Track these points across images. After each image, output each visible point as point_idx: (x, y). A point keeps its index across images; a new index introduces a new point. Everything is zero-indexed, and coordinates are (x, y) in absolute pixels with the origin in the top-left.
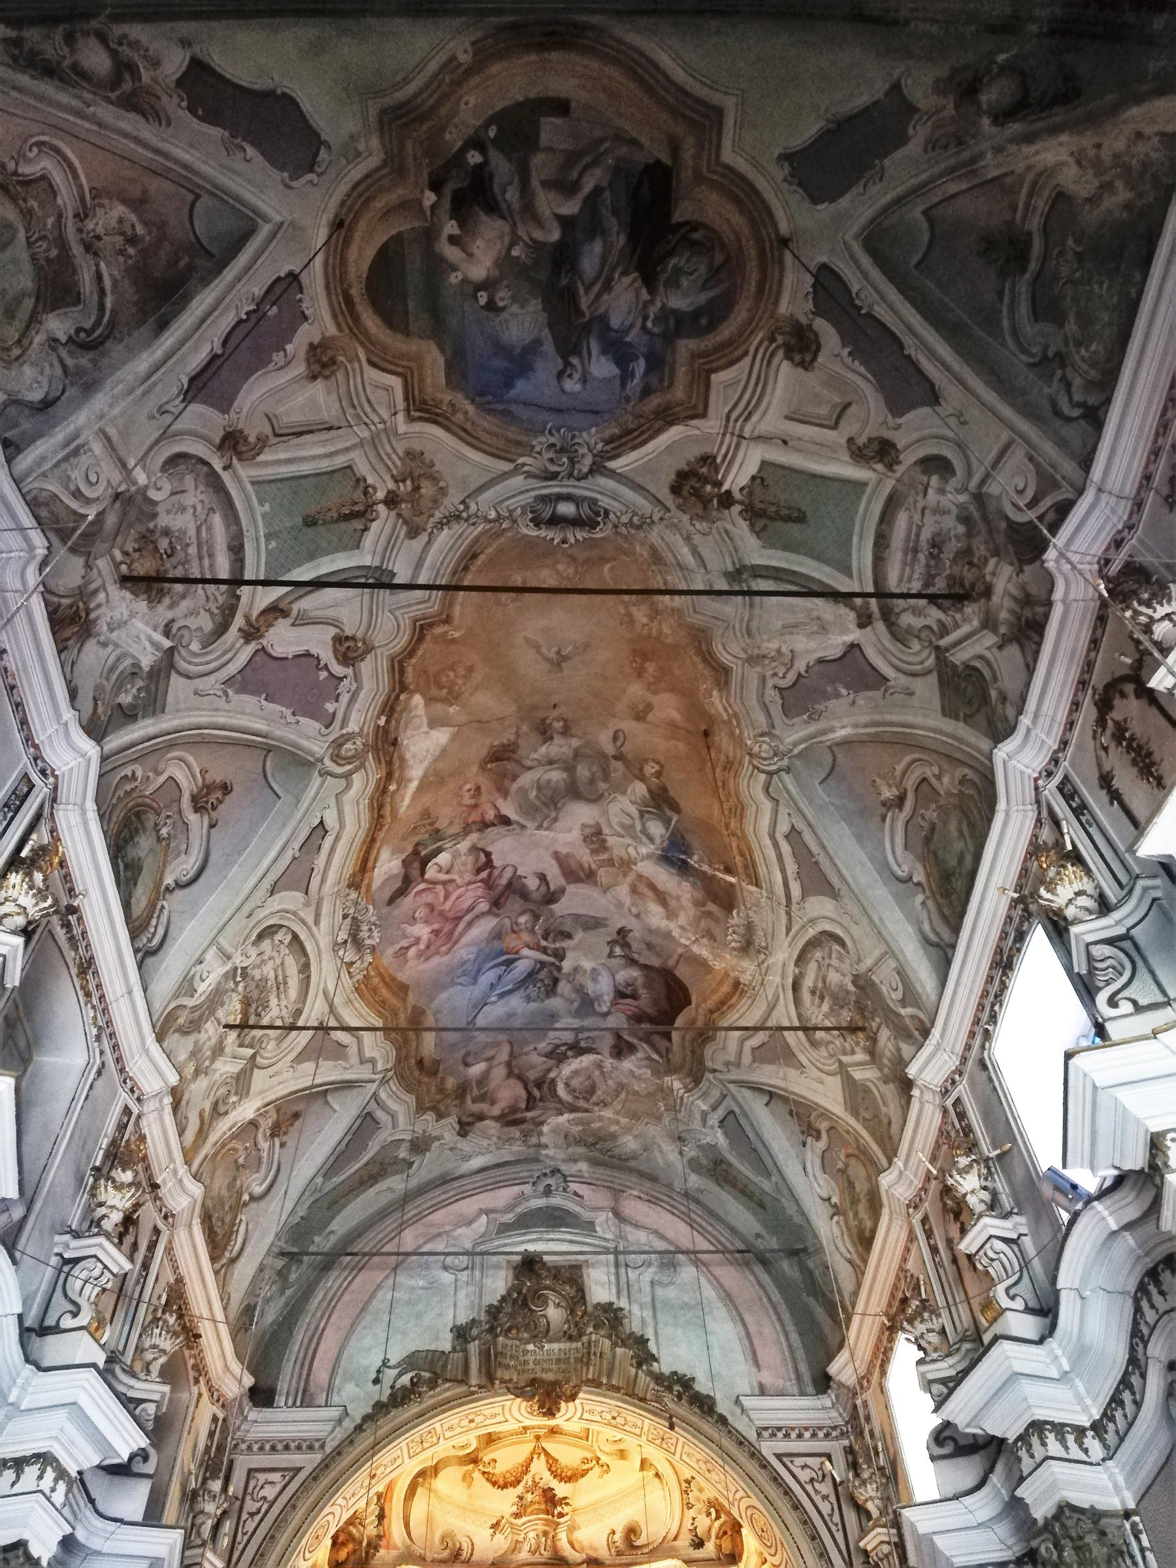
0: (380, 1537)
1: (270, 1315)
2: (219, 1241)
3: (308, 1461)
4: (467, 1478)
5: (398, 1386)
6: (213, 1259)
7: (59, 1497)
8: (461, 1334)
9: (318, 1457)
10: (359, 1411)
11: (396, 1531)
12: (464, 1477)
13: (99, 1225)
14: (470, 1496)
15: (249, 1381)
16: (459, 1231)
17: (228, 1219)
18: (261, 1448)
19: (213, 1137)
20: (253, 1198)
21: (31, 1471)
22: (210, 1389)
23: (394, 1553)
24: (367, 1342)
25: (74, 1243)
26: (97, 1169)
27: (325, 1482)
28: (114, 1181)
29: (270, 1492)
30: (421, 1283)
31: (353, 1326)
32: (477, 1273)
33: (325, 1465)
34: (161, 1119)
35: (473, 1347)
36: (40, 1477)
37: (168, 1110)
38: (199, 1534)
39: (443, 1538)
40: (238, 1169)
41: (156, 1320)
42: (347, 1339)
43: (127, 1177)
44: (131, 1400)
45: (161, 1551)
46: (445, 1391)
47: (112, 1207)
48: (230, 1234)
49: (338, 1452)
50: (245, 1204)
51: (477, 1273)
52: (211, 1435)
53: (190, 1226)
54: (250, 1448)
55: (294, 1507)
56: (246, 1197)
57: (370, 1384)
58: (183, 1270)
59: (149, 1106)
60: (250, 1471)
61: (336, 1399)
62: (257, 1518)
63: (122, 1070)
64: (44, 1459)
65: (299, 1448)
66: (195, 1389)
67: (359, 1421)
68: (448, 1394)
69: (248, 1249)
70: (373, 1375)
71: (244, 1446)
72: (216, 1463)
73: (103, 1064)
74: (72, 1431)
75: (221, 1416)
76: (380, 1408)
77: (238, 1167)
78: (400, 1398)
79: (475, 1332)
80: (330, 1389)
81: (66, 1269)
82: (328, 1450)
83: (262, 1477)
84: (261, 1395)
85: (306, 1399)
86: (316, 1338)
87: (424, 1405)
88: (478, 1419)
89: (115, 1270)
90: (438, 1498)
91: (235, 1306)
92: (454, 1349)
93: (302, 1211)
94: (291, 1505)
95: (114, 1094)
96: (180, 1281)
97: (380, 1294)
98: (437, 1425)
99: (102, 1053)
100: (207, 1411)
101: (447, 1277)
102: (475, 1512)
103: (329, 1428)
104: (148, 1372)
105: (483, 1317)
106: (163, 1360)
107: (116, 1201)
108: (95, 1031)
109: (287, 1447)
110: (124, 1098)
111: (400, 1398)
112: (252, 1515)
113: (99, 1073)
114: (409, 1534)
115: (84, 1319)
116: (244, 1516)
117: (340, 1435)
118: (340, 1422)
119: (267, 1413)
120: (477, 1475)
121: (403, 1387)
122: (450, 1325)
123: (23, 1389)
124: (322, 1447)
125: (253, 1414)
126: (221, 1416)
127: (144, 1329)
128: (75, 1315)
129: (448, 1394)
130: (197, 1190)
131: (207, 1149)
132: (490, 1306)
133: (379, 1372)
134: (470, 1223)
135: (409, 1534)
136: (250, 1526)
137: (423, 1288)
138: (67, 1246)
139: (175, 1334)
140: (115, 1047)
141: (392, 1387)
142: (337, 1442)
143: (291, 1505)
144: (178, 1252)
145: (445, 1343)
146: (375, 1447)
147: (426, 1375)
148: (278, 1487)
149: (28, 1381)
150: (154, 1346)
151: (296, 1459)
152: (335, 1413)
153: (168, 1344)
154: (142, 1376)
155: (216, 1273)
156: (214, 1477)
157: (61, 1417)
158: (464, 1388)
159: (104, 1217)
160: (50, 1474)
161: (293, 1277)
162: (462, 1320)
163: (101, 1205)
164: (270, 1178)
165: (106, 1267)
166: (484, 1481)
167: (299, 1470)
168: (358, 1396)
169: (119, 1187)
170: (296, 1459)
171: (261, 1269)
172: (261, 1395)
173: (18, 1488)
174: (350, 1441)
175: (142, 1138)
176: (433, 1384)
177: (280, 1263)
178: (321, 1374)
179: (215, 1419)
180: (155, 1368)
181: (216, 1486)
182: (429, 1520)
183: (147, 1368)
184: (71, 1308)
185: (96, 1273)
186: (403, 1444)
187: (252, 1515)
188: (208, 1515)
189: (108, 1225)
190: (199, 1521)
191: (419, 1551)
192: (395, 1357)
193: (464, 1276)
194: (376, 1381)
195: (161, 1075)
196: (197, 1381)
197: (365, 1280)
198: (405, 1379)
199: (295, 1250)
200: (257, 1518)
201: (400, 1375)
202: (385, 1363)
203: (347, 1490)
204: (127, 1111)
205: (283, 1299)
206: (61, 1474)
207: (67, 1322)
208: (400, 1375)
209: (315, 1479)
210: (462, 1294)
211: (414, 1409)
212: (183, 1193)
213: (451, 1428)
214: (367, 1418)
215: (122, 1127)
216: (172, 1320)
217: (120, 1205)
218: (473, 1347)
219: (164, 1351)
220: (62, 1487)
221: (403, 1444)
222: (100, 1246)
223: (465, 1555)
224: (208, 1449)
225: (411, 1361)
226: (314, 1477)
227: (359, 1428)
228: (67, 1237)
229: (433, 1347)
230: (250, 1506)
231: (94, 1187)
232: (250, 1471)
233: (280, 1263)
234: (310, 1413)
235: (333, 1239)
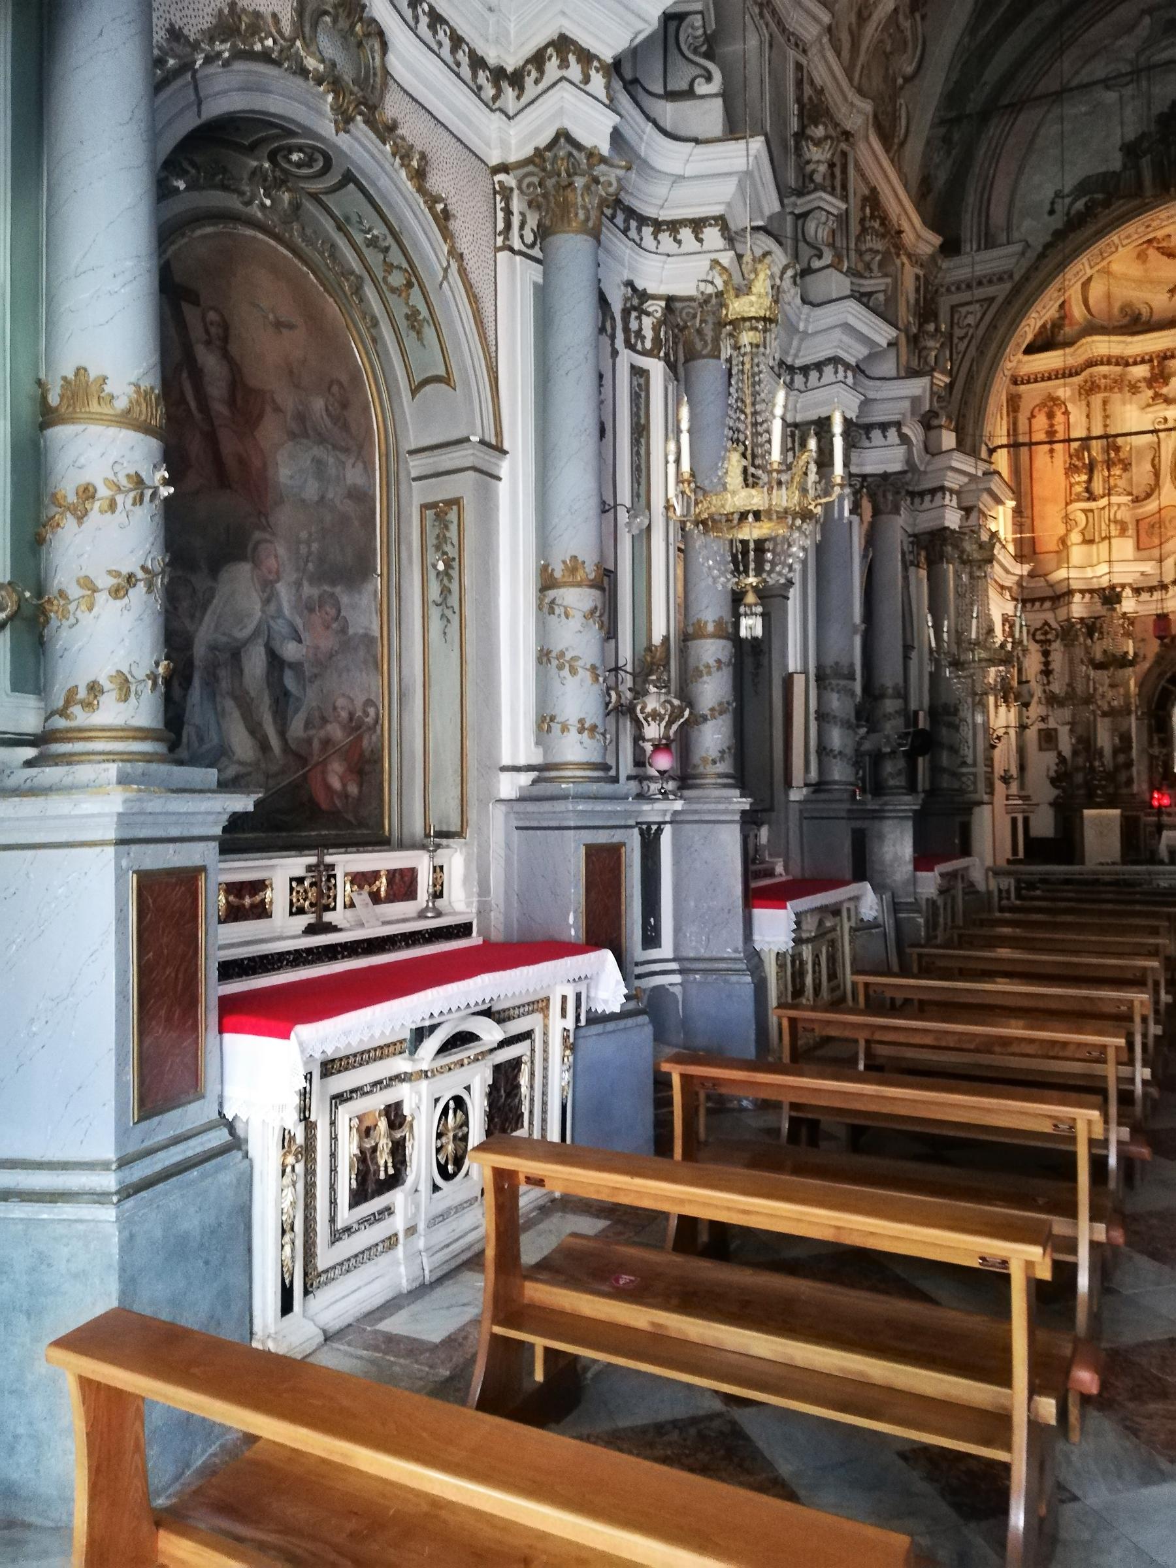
0: (1063, 318)
1: (941, 178)
2: (886, 130)
3: (1001, 291)
4: (1142, 257)
5: (1073, 212)
6: (887, 151)
7: (850, 381)
8: (1131, 150)
9: (1008, 286)
10: (1039, 241)
11: (1078, 312)
12: (1139, 256)
13: (812, 180)
14: (1146, 271)
15: (937, 240)
16: (1120, 42)
17: (889, 109)
18: (958, 288)
19: (864, 45)
20: (907, 80)
21: (829, 370)
22: (909, 256)
23: (1076, 328)
24: (1037, 179)
25: (800, 201)
26: (796, 135)
27: (1016, 306)
28: (812, 139)
29: (970, 320)
30: (1083, 109)
31: (1021, 170)
32: (1144, 83)
33: (1016, 291)
34: (824, 57)
35: (1145, 162)
36: (836, 372)
37: (827, 46)
38: (926, 363)
39: (1122, 309)
40: (887, 58)
41: (864, 230)
42: (1017, 181)
43: (819, 131)
44: (863, 294)
45: (917, 392)
46: (1119, 207)
47: (818, 162)
48: (895, 118)
49: (1026, 278)
50: (902, 88)
51: (1144, 83)
52: (917, 290)
53: (867, 138)
54: (948, 290)
55: (995, 327)
56: (900, 81)
57: (1046, 216)
58: (874, 183)
59: (813, 51)
60: (953, 309)
61: (1016, 235)
62: (966, 341)
63: (784, 30)
64: (835, 361)
65: (990, 282)
66: (898, 262)
67: (1040, 249)
68: (1124, 208)
69: (913, 128)
70: (1047, 207)
71: (943, 290)
72: (926, 311)
73: (771, 35)
74: (846, 339)
75: (921, 273)
76: (1059, 235)
77: (887, 56)
78: (1075, 223)
79: (1145, 145)
80: (1009, 228)
81: (800, 222)
82: (1017, 277)
83: (963, 310)
84: (951, 247)
85: (988, 241)
86: (988, 186)
87: (1100, 225)
88: (1154, 224)
89: (835, 212)
90: (1115, 277)
91: (914, 182)
92: (1125, 166)
93: (955, 76)
94: (993, 326)
95: (785, 57)
96: (874, 190)
97: (1043, 131)
98: (1115, 238)
99: (767, 25)
100: (909, 274)
101: (1111, 97)
102: (1151, 282)
103: (1014, 260)
104: (871, 271)
105: (1153, 128)
106: (878, 258)
107: (818, 155)
108: (757, 10)
109: (980, 283)
110: (792, 54)
111: (1075, 223)
112: (961, 339)
113: (771, 46)
114: (1089, 310)
115: (828, 258)
116: (956, 340)
117: (1025, 263)
118: (1023, 254)
119: (956, 261)
120: (1152, 253)
121: (1079, 213)
122: (1119, 144)
123: (807, 321)
124: (1011, 276)
125: (945, 264)
126: (921, 273)
127: (858, 238)
128: (820, 257)
129: (1124, 208)
130: (867, 106)
131: (862, 58)
132: (1161, 115)
133: (1053, 203)
134: (1130, 28)
135: (1089, 310)
136: (962, 346)
137: (1086, 114)
138: (795, 205)
139: (883, 236)
140: (774, 13)
141: (1068, 214)
142: (1023, 271)
143: (993, 326)
144: (862, 162)
145: (1116, 163)
146: (1061, 266)
147: (1099, 196)
148: (979, 315)
149: (808, 315)
150: (871, 250)
151: (990, 291)
152: (1017, 248)
153: (879, 245)
154: (867, 274)
155: (892, 161)
156: (927, 321)
157: (838, 334)
158: (1137, 202)
159: (813, 172)
160: (841, 369)
161: (956, 137)
162: (1131, 136)
163: (808, 162)
164: (918, 53)
165: (829, 213)
166: (1159, 256)
167: (991, 300)
168: (1035, 229)
169: (818, 143)
170: (990, 291)
171: (928, 143)
172: (951, 247)
173: (824, 381)
174: (1034, 267)
175: (821, 92)
176: (1107, 204)
177: (942, 131)
178: (998, 215)
179: (917, 277)
180: (875, 266)
181: (931, 327)
182: (1109, 296)
183: (868, 267)
184: (814, 252)
185: (823, 219)
186: (1085, 260)
187: (961, 339)
188: (931, 349)
189: (818, 178)
190: (924, 353)
191: (1098, 321)
192: (1069, 185)
193: (1129, 91)
194: (1052, 212)
195: (816, 19)
196: (898, 255)
197: (1026, 120)
198: (1080, 205)
199: (953, 114)
200: (966, 341)
201: (1072, 203)
202: (1058, 195)
203: (1038, 306)
204: (799, 67)
205: (949, 162)
206: (847, 366)
207: (816, 264)
208: (1072, 203)
209: (1009, 303)
210: (1128, 111)
211: (1090, 230)
212: (855, 113)
213: (1128, 237)
214: (1048, 246)
215: (799, 83)
216: (876, 225)
217: (823, 158)
218: (1145, 162)
219: (877, 252)
220: (850, 374)
221: (1085, 260)
222: (821, 198)
223: (1144, 318)
224: (917, 301)
225: (1082, 188)
226: (1008, 301)
227: (1042, 256)
228: (793, 199)
229: (1103, 169)
230: (958, 332)
231: (798, 148)
232: (953, 309)
233: (942, 131)
234: (995, 253)
235: (987, 89)
